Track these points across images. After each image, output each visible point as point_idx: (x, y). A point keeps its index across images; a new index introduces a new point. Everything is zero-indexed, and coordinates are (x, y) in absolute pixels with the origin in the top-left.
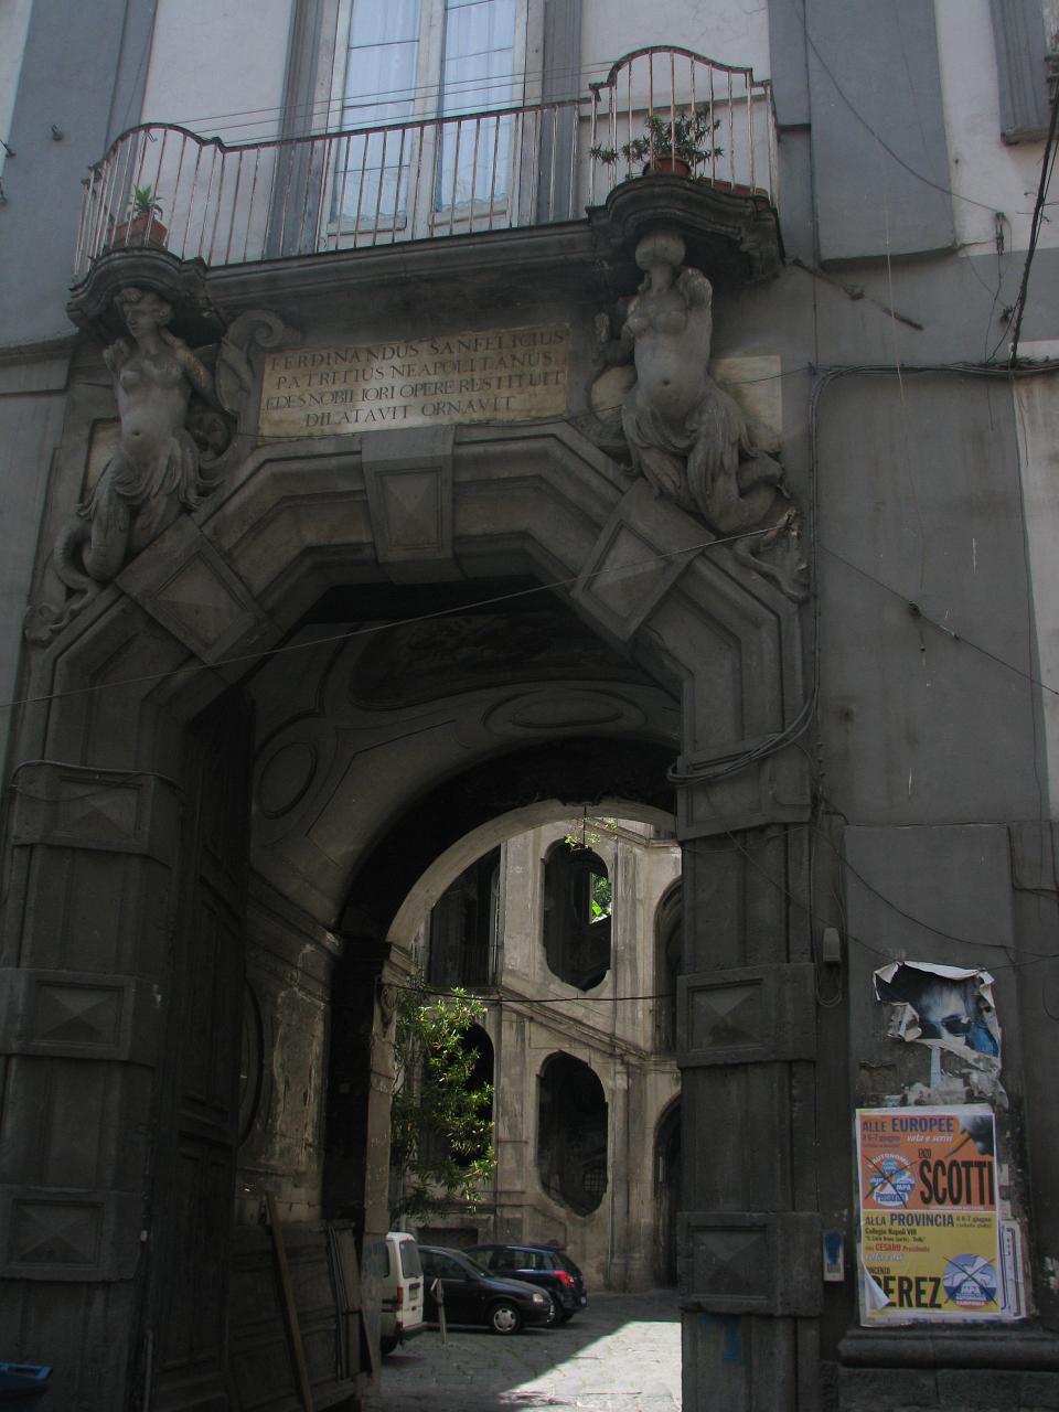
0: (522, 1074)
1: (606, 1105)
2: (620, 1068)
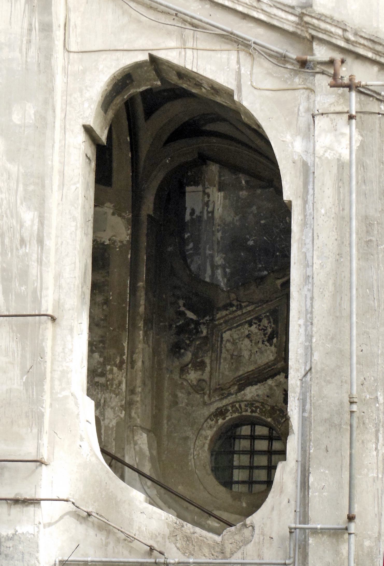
0: (43, 123)
1: (286, 210)
2: (325, 96)
